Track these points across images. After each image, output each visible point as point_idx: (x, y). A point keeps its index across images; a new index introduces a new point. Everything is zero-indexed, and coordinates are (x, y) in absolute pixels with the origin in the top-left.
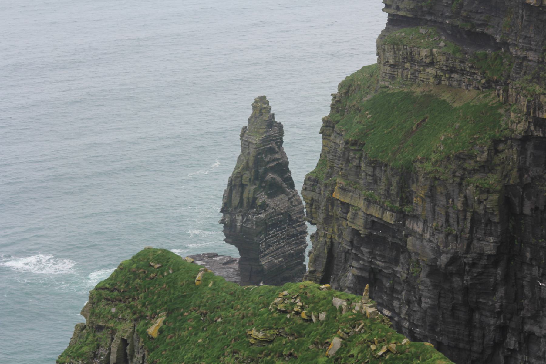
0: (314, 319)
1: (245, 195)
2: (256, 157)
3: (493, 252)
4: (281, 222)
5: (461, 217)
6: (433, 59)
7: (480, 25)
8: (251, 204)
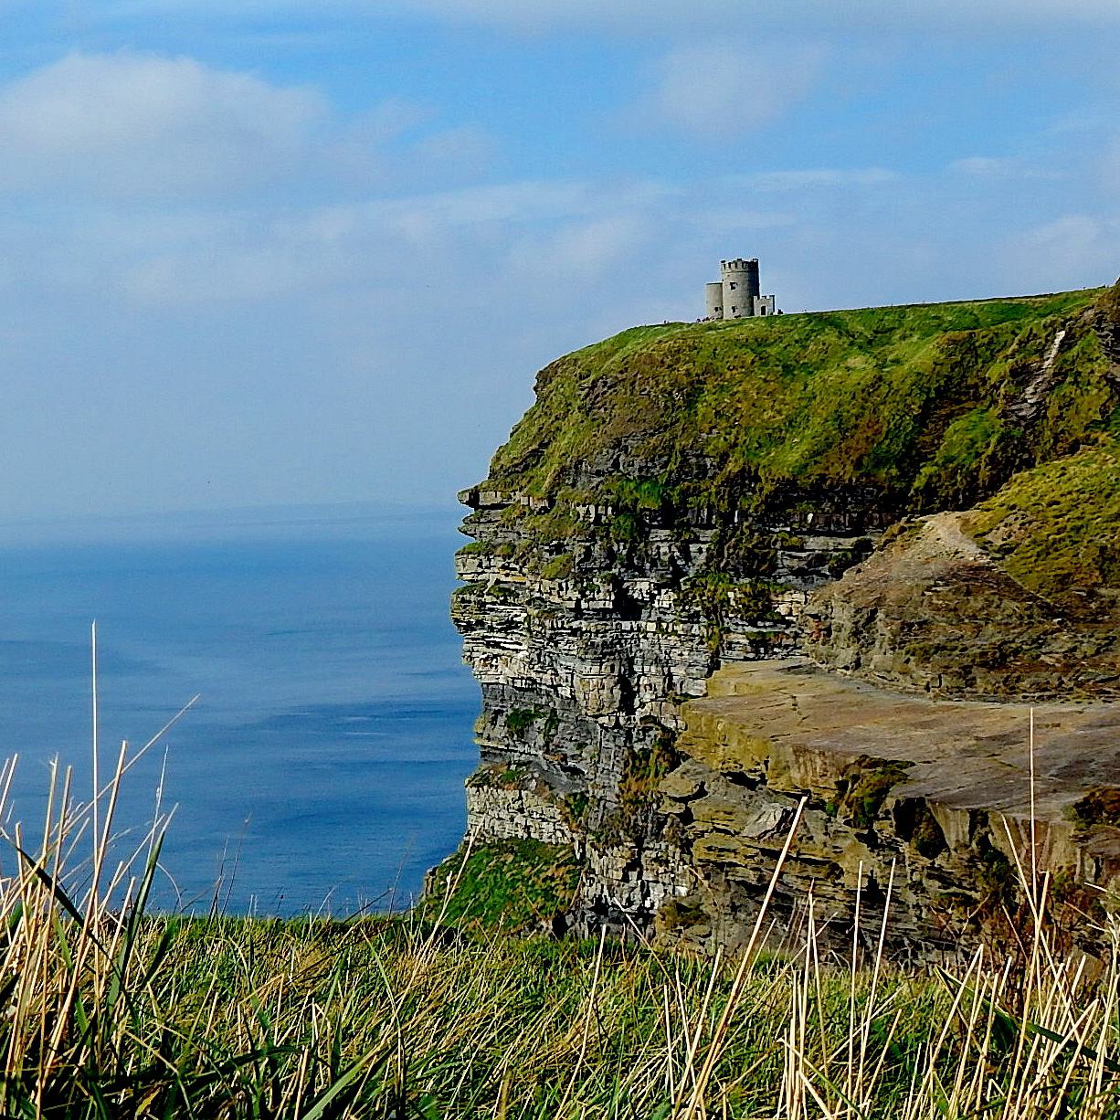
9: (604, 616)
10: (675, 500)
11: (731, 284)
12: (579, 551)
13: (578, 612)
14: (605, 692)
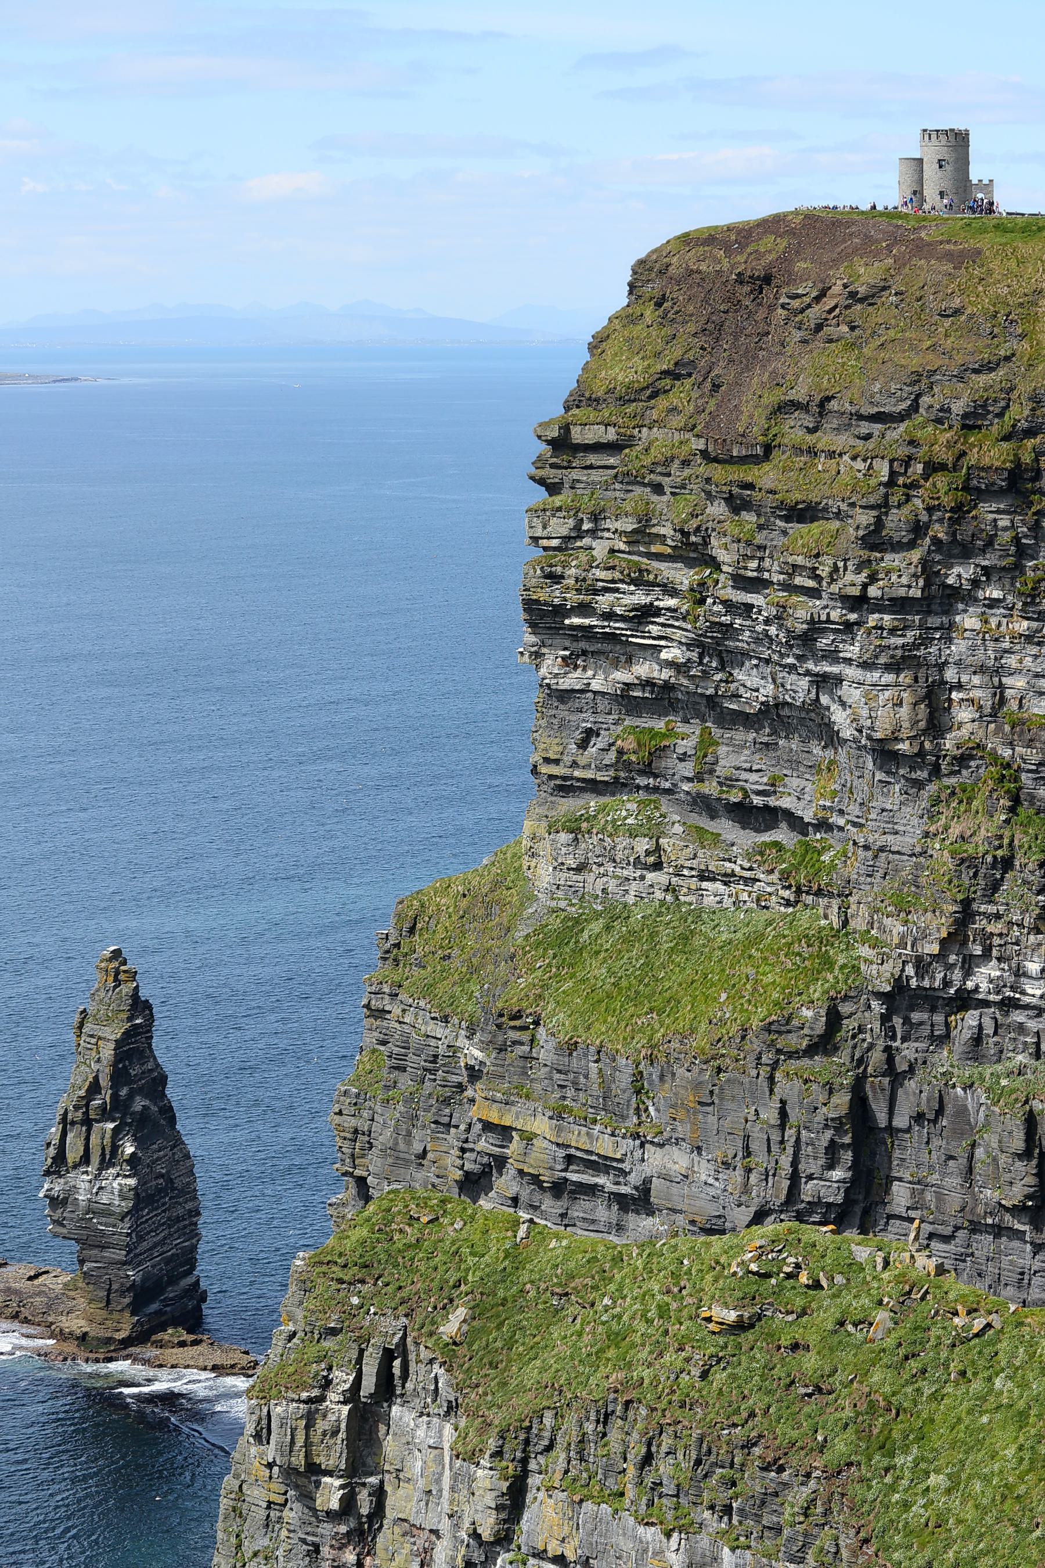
0: (824, 1283)
1: (94, 1140)
2: (114, 1065)
3: (839, 1199)
4: (160, 1191)
5: (775, 1137)
6: (660, 857)
7: (759, 793)
8: (108, 1157)
9: (903, 606)
10: (1027, 458)
11: (939, 160)
12: (865, 518)
13: (859, 602)
14: (904, 711)
